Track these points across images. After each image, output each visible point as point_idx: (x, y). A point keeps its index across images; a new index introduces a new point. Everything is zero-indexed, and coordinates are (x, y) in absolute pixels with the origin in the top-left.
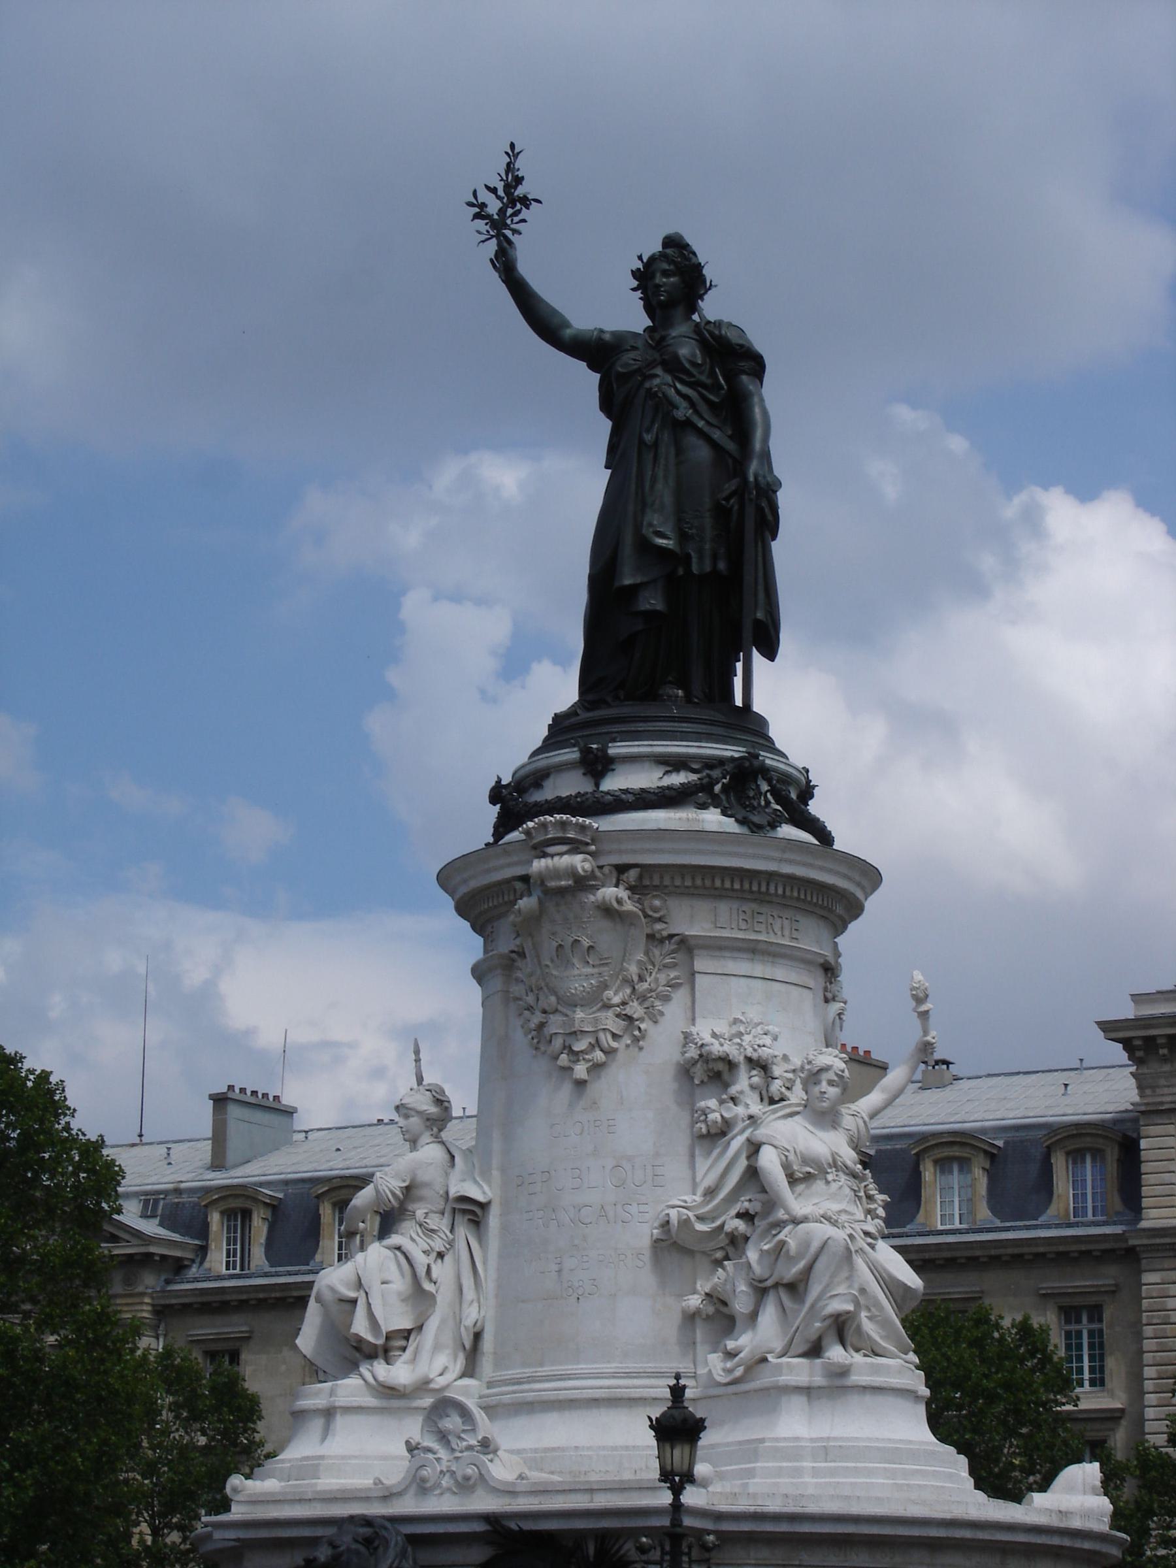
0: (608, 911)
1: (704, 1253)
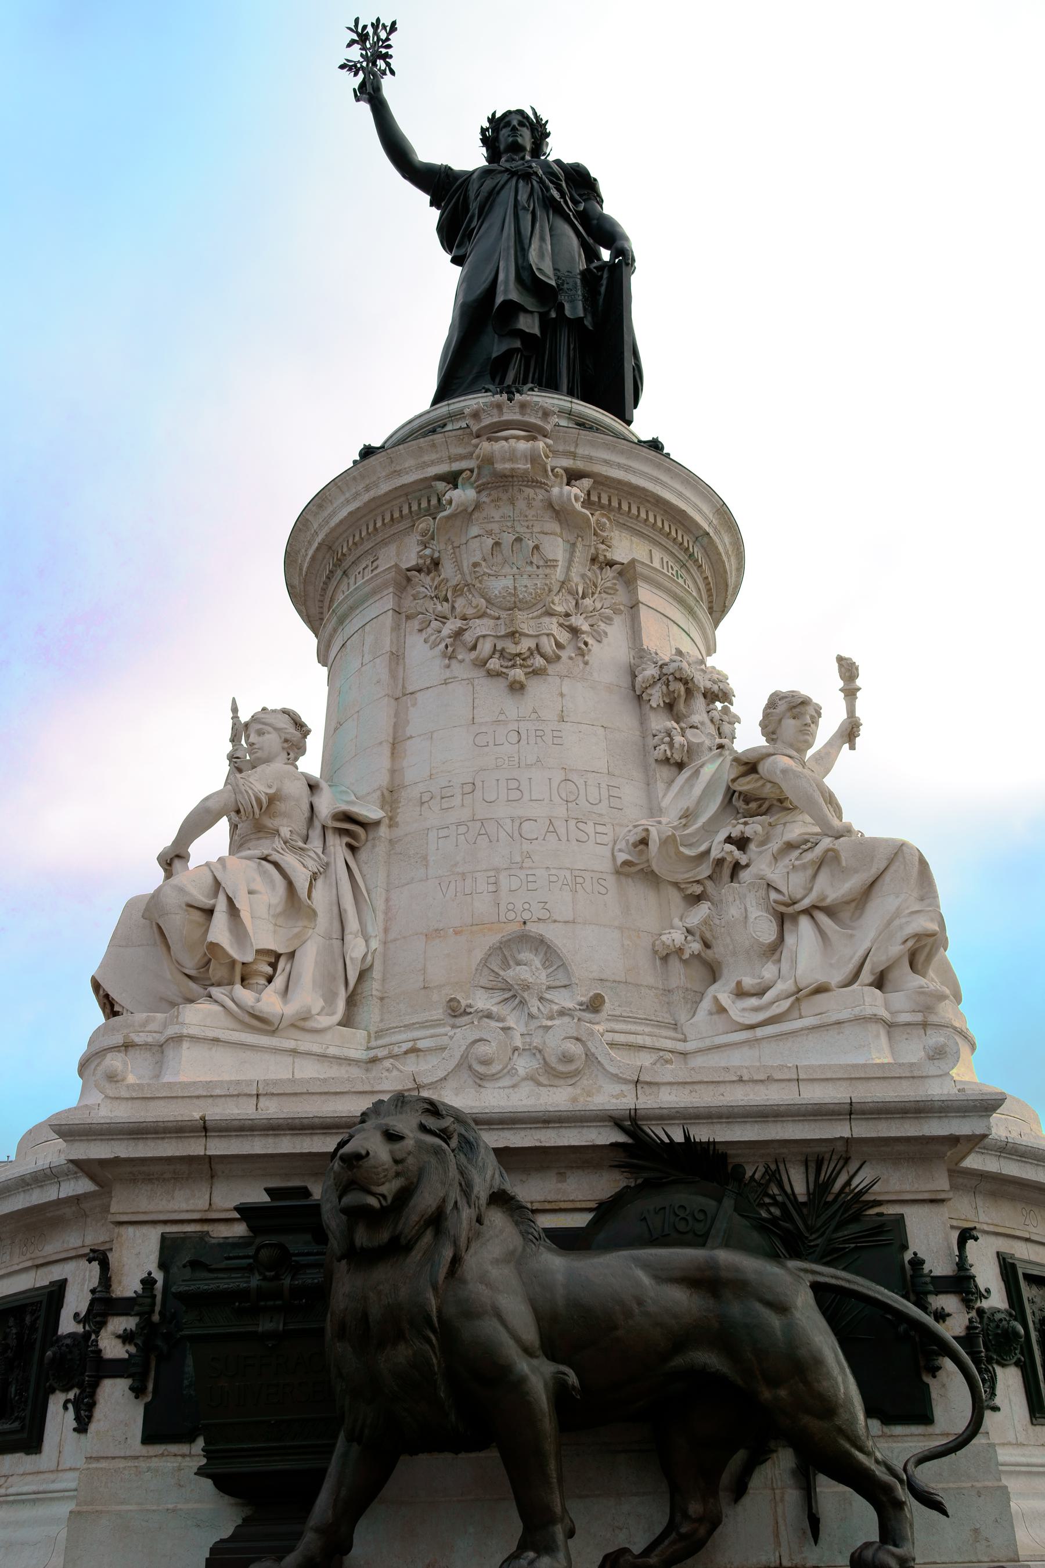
0: (560, 513)
1: (676, 885)
